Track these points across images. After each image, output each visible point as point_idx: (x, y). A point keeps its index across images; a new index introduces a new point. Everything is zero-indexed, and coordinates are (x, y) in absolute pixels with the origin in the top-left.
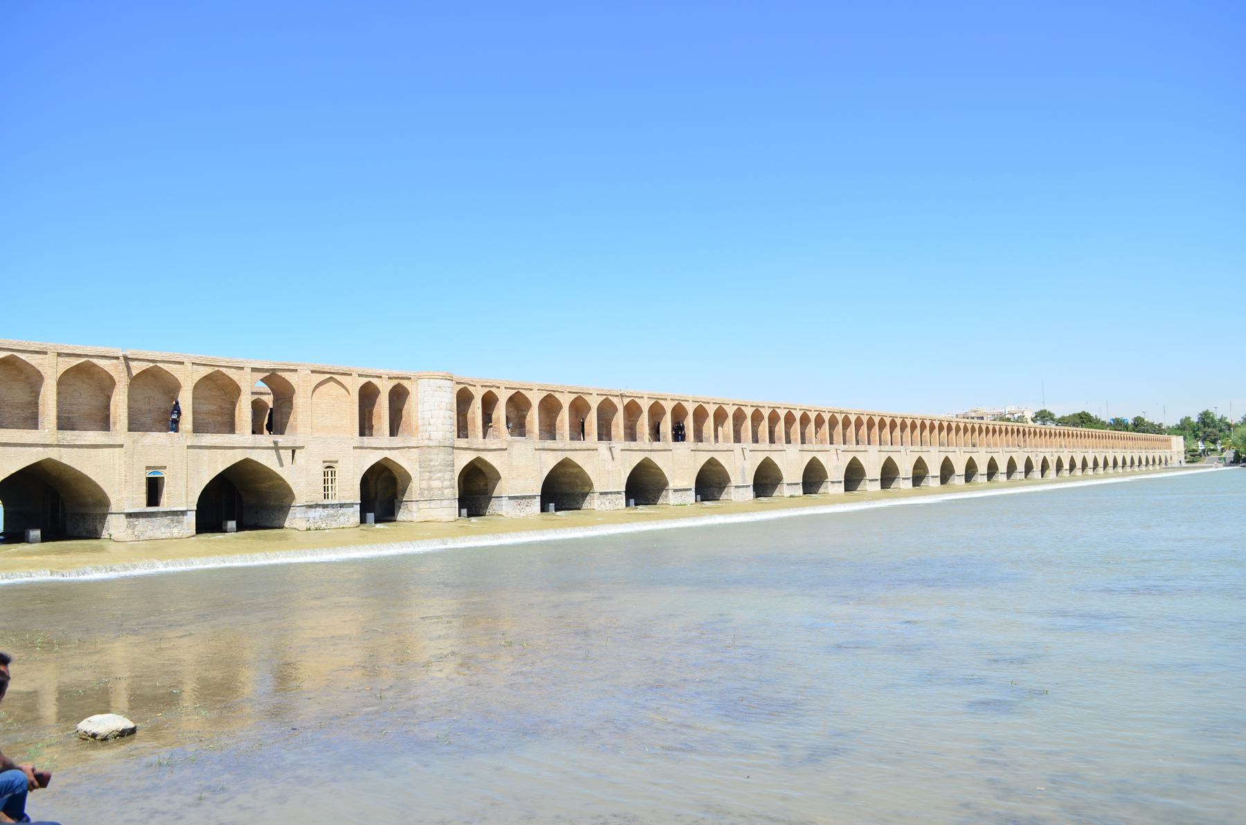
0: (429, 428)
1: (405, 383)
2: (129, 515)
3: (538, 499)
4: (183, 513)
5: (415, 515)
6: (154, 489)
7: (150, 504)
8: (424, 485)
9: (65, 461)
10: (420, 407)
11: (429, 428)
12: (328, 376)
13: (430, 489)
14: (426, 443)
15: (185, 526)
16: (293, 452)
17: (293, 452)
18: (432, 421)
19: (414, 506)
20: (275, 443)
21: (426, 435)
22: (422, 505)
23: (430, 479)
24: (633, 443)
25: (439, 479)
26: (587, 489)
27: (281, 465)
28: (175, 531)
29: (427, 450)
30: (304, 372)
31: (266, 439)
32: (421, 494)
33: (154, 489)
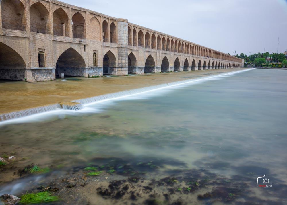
0: (122, 40)
1: (115, 23)
2: (33, 70)
3: (144, 68)
4: (51, 69)
5: (117, 73)
6: (41, 58)
7: (40, 66)
8: (120, 62)
9: (7, 44)
10: (119, 32)
11: (122, 40)
12: (94, 16)
13: (122, 63)
14: (121, 46)
15: (52, 76)
16: (85, 46)
17: (85, 46)
18: (123, 38)
19: (116, 69)
20: (79, 41)
21: (121, 43)
22: (119, 69)
23: (122, 59)
24: (164, 51)
25: (124, 60)
26: (153, 66)
27: (81, 51)
28: (49, 77)
29: (121, 49)
30: (88, 13)
31: (77, 40)
32: (119, 65)
33: (41, 58)
